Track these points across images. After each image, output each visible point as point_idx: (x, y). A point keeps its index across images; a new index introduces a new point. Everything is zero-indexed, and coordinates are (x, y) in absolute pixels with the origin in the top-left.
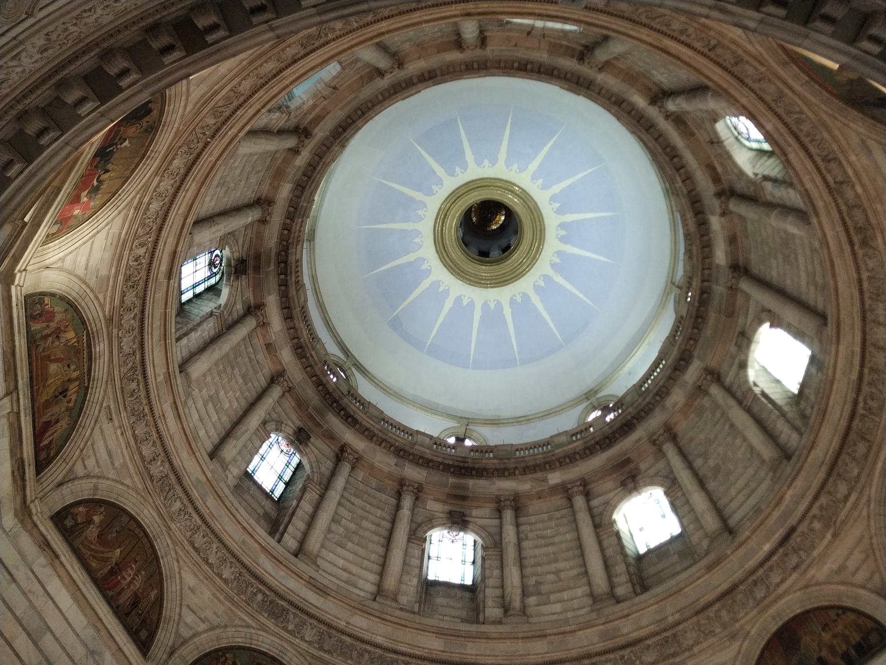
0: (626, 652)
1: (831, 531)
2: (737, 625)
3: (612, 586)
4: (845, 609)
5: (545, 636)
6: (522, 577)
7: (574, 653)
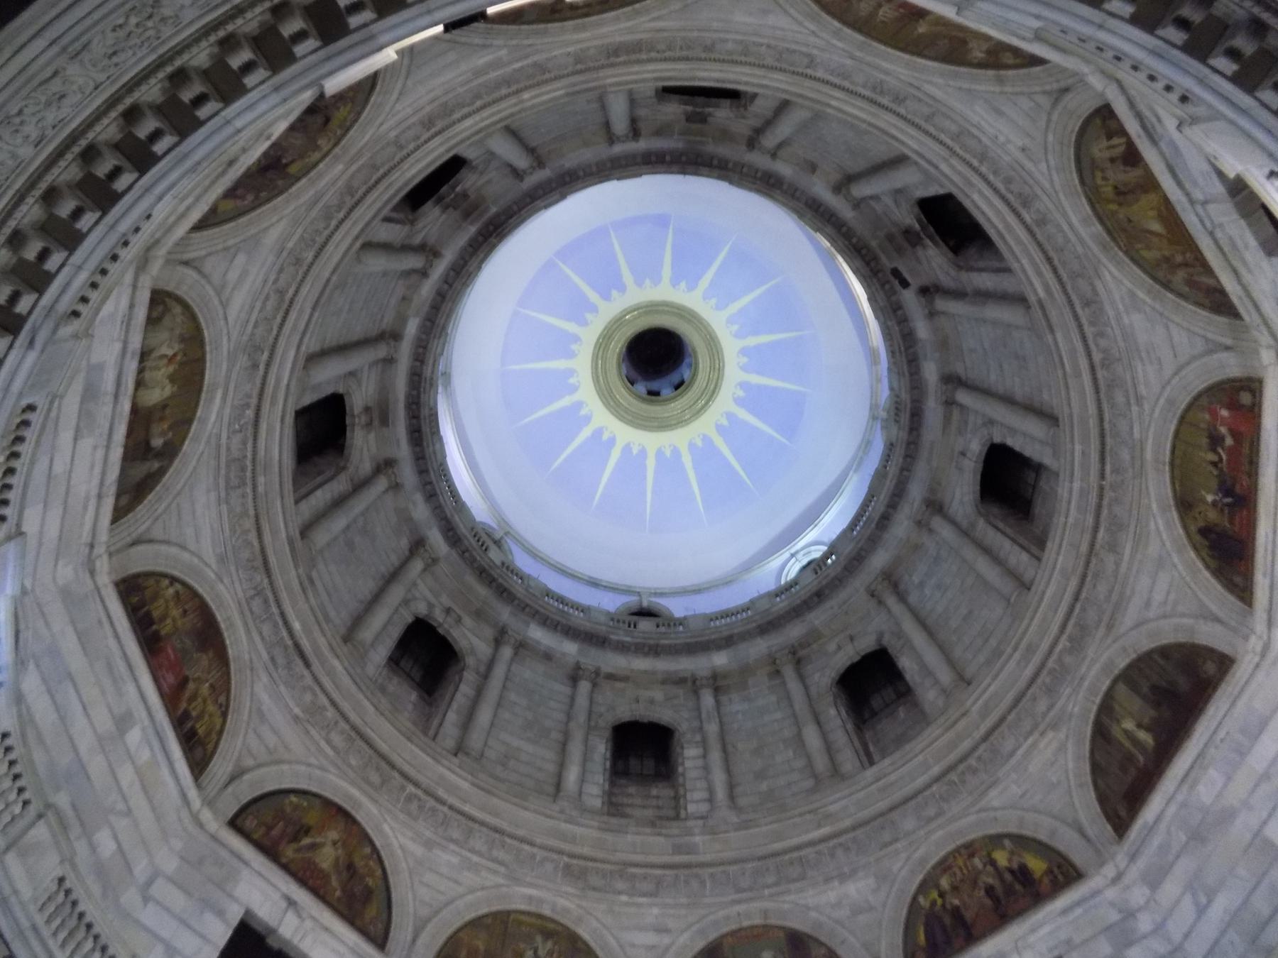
1: (301, 715)
4: (224, 715)
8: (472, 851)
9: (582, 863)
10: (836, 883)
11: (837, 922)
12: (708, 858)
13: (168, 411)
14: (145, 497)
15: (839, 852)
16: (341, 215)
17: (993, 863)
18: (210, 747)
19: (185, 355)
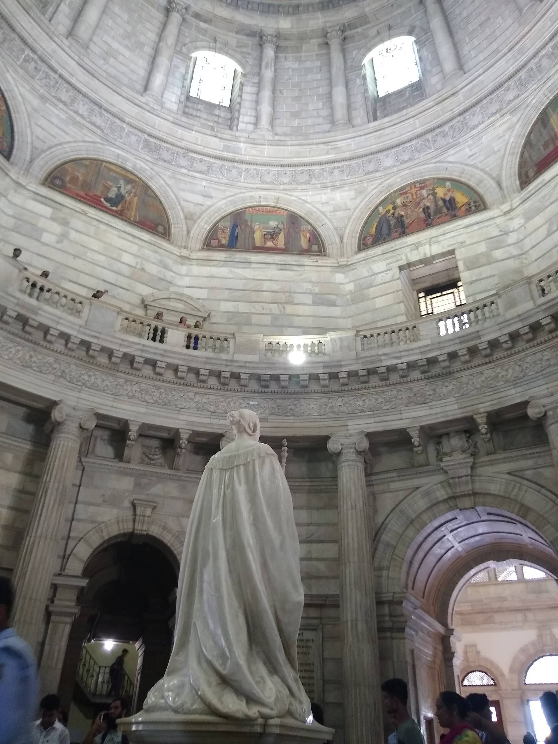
8: (76, 112)
9: (158, 142)
10: (329, 190)
11: (322, 213)
12: (247, 158)
15: (336, 172)
17: (434, 194)
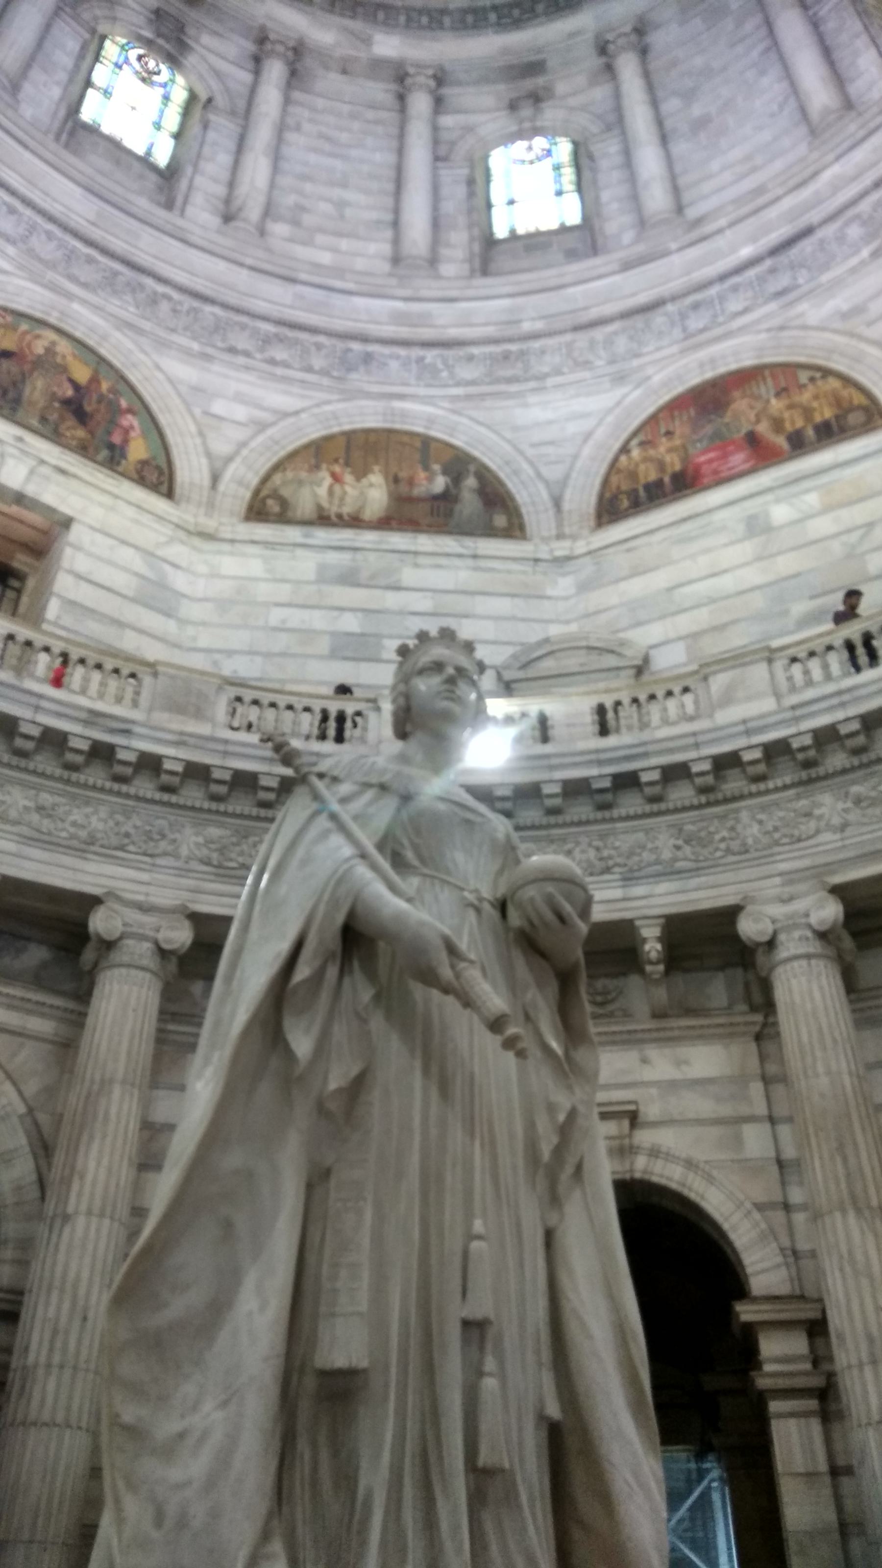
0: (430, 355)
2: (635, 363)
3: (433, 261)
4: (827, 373)
5: (293, 281)
6: (272, 185)
7: (340, 325)
13: (403, 474)
14: (508, 493)
16: (149, 282)
18: (859, 399)
19: (336, 461)
